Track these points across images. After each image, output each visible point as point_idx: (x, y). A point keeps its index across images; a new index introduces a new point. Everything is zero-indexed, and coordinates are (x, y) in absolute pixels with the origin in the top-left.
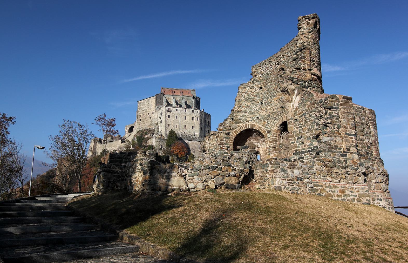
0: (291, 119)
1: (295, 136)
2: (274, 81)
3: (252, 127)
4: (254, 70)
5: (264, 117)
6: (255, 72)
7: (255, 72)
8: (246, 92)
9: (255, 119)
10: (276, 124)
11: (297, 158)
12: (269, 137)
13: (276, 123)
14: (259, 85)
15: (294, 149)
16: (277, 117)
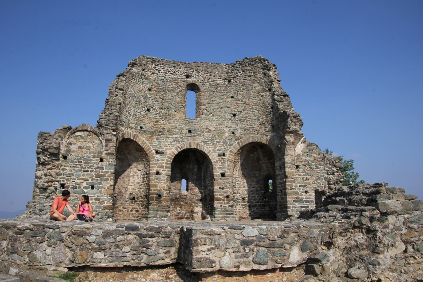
0: (292, 164)
1: (296, 182)
2: (178, 93)
3: (134, 138)
4: (143, 61)
5: (152, 130)
6: (145, 65)
7: (145, 65)
8: (132, 86)
9: (139, 128)
10: (175, 146)
11: (300, 206)
12: (160, 159)
13: (175, 145)
14: (147, 84)
15: (295, 196)
16: (179, 139)
